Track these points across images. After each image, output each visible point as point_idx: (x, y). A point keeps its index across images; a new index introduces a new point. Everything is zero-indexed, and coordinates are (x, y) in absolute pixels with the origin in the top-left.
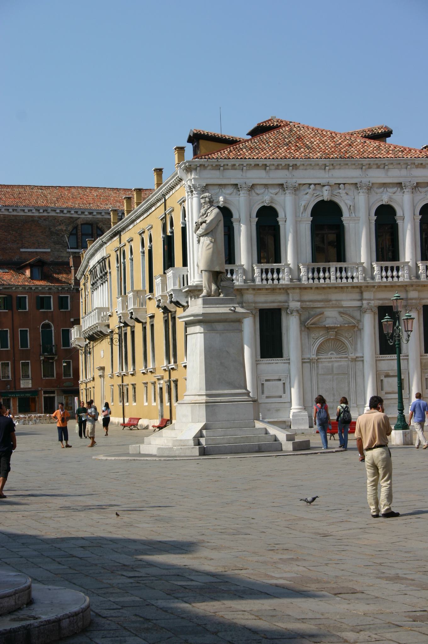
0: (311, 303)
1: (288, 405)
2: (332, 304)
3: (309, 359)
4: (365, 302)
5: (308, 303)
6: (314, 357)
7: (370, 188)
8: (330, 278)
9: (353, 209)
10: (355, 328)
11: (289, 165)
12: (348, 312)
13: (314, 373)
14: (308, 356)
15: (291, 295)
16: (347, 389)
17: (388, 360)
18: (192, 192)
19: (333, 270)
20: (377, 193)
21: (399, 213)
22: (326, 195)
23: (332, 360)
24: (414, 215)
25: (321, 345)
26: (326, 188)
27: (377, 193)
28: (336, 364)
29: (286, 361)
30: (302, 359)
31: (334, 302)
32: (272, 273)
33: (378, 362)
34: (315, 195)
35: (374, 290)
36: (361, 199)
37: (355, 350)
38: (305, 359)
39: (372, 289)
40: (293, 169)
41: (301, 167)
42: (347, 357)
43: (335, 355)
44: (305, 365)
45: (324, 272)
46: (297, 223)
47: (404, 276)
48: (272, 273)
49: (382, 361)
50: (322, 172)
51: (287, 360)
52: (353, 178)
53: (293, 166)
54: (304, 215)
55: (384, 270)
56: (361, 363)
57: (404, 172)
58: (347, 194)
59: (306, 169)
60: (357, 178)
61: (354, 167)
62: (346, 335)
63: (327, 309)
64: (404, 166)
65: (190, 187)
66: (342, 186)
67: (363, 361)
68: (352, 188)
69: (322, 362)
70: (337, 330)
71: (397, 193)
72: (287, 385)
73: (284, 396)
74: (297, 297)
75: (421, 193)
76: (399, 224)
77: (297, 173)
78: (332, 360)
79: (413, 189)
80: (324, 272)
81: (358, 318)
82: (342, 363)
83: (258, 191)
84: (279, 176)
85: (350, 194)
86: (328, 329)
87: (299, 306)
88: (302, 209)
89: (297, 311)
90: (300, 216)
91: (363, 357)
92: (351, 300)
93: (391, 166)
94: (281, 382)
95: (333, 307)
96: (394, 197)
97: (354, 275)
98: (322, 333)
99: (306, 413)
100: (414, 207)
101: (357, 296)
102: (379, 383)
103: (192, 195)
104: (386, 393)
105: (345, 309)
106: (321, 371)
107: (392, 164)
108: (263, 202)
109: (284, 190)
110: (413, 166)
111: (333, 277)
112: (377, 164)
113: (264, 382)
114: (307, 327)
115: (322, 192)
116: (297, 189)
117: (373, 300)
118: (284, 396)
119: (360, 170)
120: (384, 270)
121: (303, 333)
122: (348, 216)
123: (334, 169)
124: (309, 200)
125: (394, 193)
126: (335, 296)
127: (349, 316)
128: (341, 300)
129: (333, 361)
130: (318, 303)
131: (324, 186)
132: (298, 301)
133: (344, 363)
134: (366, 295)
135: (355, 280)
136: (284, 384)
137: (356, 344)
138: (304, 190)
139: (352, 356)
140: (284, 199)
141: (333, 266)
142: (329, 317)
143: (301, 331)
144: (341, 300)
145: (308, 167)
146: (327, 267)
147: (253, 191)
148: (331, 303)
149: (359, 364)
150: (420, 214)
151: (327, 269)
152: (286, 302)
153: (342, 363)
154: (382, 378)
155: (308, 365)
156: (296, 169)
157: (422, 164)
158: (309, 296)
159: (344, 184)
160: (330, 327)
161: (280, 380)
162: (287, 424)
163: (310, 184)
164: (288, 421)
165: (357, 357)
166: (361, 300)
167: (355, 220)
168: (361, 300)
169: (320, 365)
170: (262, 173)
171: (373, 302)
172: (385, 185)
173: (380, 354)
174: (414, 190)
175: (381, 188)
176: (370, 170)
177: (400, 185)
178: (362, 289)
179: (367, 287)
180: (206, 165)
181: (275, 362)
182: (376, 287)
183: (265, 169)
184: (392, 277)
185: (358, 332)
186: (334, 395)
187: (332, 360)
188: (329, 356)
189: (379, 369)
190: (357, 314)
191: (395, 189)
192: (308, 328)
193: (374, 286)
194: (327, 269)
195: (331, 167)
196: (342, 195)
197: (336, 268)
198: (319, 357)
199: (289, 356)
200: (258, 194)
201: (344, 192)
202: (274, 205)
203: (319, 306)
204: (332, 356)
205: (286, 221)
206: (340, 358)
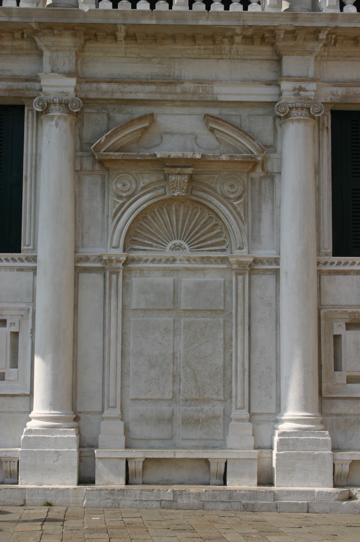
0: (114, 86)
1: (20, 403)
2: (184, 92)
3: (100, 259)
4: (286, 86)
5: (104, 86)
6: (119, 251)
10: (257, 168)
12: (236, 120)
13: (115, 305)
14: (99, 251)
15: (47, 54)
16: (220, 362)
23: (177, 265)
25: (142, 217)
28: (187, 281)
30: (78, 260)
31: (188, 86)
33: (325, 278)
35: (318, 48)
37: (254, 238)
38: (87, 259)
39: (310, 45)
42: (224, 260)
43: (188, 253)
44: (85, 278)
49: (340, 278)
51: (28, 259)
56: (271, 279)
62: (226, 188)
63: (168, 109)
67: (277, 272)
69: (141, 270)
70: (194, 170)
72: (24, 341)
73: (11, 373)
74: (66, 61)
78: (177, 265)
81: (268, 138)
82: (209, 278)
86: (166, 165)
87: (72, 90)
89: (64, 104)
91: (277, 261)
92: (244, 81)
94: (8, 330)
95: (185, 103)
98: (145, 180)
99: (72, 435)
101: (265, 71)
102: (328, 347)
104: (350, 380)
105: (226, 111)
106: (136, 301)
114: (96, 160)
117: (313, 80)
118: (11, 373)
121: (87, 180)
126: (193, 68)
127: (239, 129)
128: (211, 82)
129: (178, 270)
130: (139, 87)
132: (69, 74)
133: (214, 277)
134: (292, 65)
136: (15, 335)
137: (257, 219)
139: (243, 255)
142: (172, 134)
143: (78, 173)
144: (211, 82)
148: (179, 89)
149: (263, 283)
152: (36, 79)
153: (209, 278)
154: (339, 329)
155: (97, 278)
158: (112, 64)
160: (169, 159)
162: (6, 466)
164: (9, 460)
165: (255, 261)
166: (275, 83)
168: (275, 83)
169: (136, 281)
171: (312, 86)
173: (335, 254)
178: (280, 44)
179: (293, 33)
182: (322, 36)
185: (266, 184)
186: (175, 378)
187: (171, 268)
188: (168, 253)
189: (327, 301)
190: (262, 126)
192: (101, 162)
193: (317, 31)
198: (134, 254)
203: (141, 96)
204: (176, 254)
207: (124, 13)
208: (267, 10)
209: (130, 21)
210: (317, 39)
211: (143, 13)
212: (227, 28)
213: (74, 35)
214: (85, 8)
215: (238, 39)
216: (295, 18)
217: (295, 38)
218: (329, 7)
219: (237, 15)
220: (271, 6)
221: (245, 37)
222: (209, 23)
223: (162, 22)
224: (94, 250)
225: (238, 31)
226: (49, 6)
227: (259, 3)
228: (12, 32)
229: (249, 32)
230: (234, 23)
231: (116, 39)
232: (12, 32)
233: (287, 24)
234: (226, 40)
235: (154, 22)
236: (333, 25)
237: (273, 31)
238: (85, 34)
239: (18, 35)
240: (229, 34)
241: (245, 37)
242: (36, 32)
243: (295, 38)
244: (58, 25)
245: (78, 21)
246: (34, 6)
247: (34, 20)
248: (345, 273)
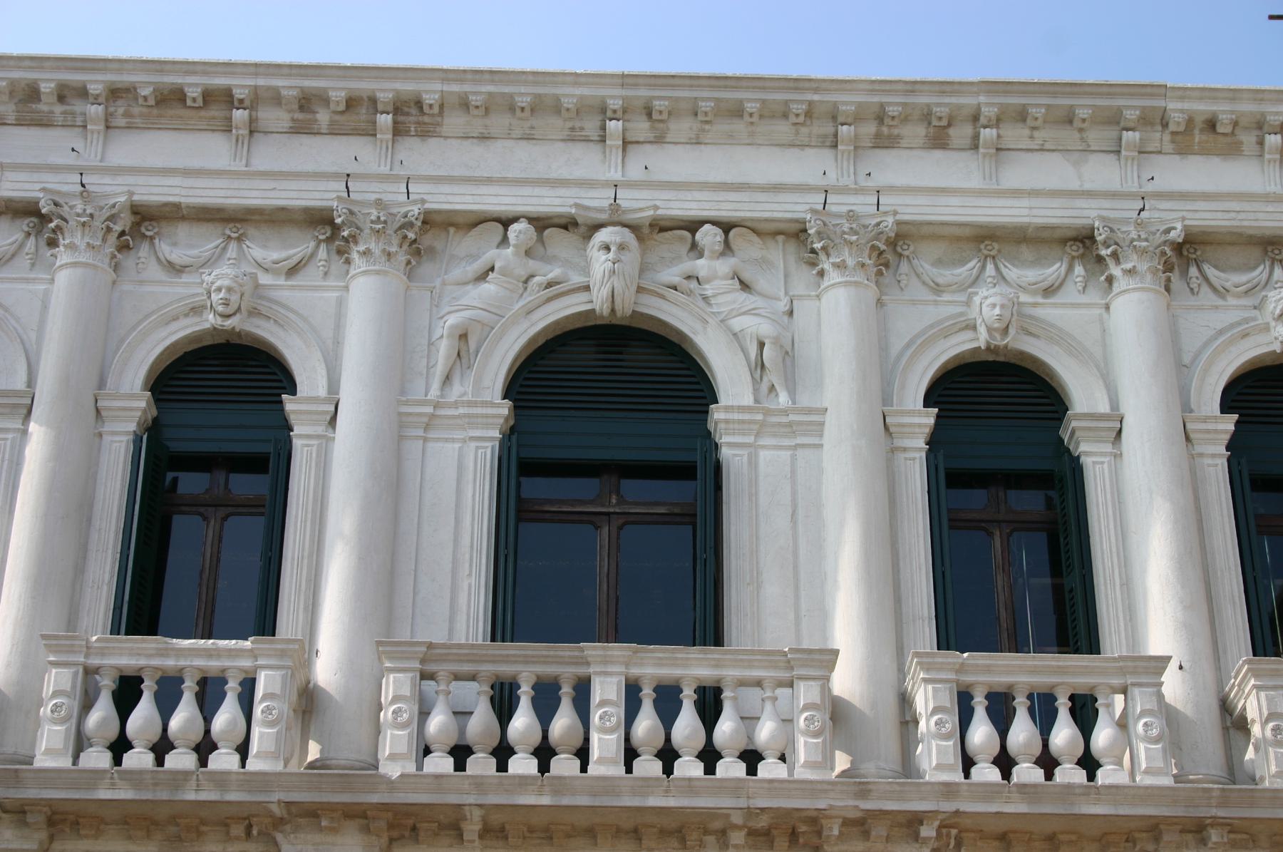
7: (891, 250)
8: (583, 754)
9: (777, 362)
11: (373, 101)
19: (607, 691)
21: (1084, 396)
22: (599, 280)
24: (1186, 408)
26: (603, 235)
27: (937, 289)
36: (833, 313)
40: (398, 131)
41: (454, 122)
45: (545, 706)
46: (402, 429)
47: (1134, 761)
48: (166, 705)
52: (778, 188)
53: (398, 109)
54: (456, 391)
55: (980, 714)
57: (1102, 173)
58: (745, 286)
59: (484, 138)
61: (783, 129)
66: (709, 236)
68: (779, 254)
75: (1221, 292)
76: (1086, 461)
77: (419, 156)
79: (1168, 268)
80: (545, 706)
83: (176, 255)
88: (444, 349)
90: (434, 392)
93: (1014, 134)
96: (1049, 312)
97: (765, 732)
100: (1179, 370)
107: (1022, 116)
109: (340, 252)
110: (1157, 137)
111: (604, 745)
112: (927, 117)
115: (586, 270)
116: (425, 237)
119: (828, 153)
120: (980, 714)
122: (748, 400)
123: (659, 140)
124: (505, 308)
131: (598, 227)
135: (769, 769)
138: (473, 257)
140: (341, 304)
141: (609, 669)
145: (499, 122)
146: (567, 674)
147: (144, 250)
150: (1226, 407)
151: (566, 691)
156: (425, 133)
157: (1211, 125)
159: (726, 227)
163: (506, 222)
167: (792, 429)
170: (211, 150)
172: (989, 241)
174: (1175, 277)
175: (963, 262)
176: (888, 157)
177: (1082, 244)
182: (927, 831)
184: (1048, 762)
191: (1054, 271)
193: (913, 822)
194: (566, 691)
195: (641, 128)
196: (709, 290)
200: (175, 269)
201: (724, 266)
205: (333, 421)
207: (479, 783)
208: (801, 773)
209: (493, 799)
210: (916, 837)
211: (523, 780)
212: (712, 814)
213: (366, 830)
214: (392, 770)
215: (737, 838)
216: (863, 791)
217: (866, 835)
218: (939, 767)
219: (733, 786)
220: (808, 765)
221: (752, 833)
222: (671, 802)
223: (565, 801)
225: (737, 819)
226: (312, 766)
227: (783, 758)
228: (225, 824)
229: (762, 822)
230: (725, 802)
231: (460, 837)
232: (225, 824)
233: (847, 804)
234: (710, 839)
235: (545, 800)
236: (948, 806)
237: (815, 820)
238: (391, 826)
239: (237, 830)
240: (717, 825)
241: (752, 833)
242: (279, 823)
243: (866, 835)
244: (330, 808)
245: (375, 798)
246: (279, 767)
247: (275, 797)
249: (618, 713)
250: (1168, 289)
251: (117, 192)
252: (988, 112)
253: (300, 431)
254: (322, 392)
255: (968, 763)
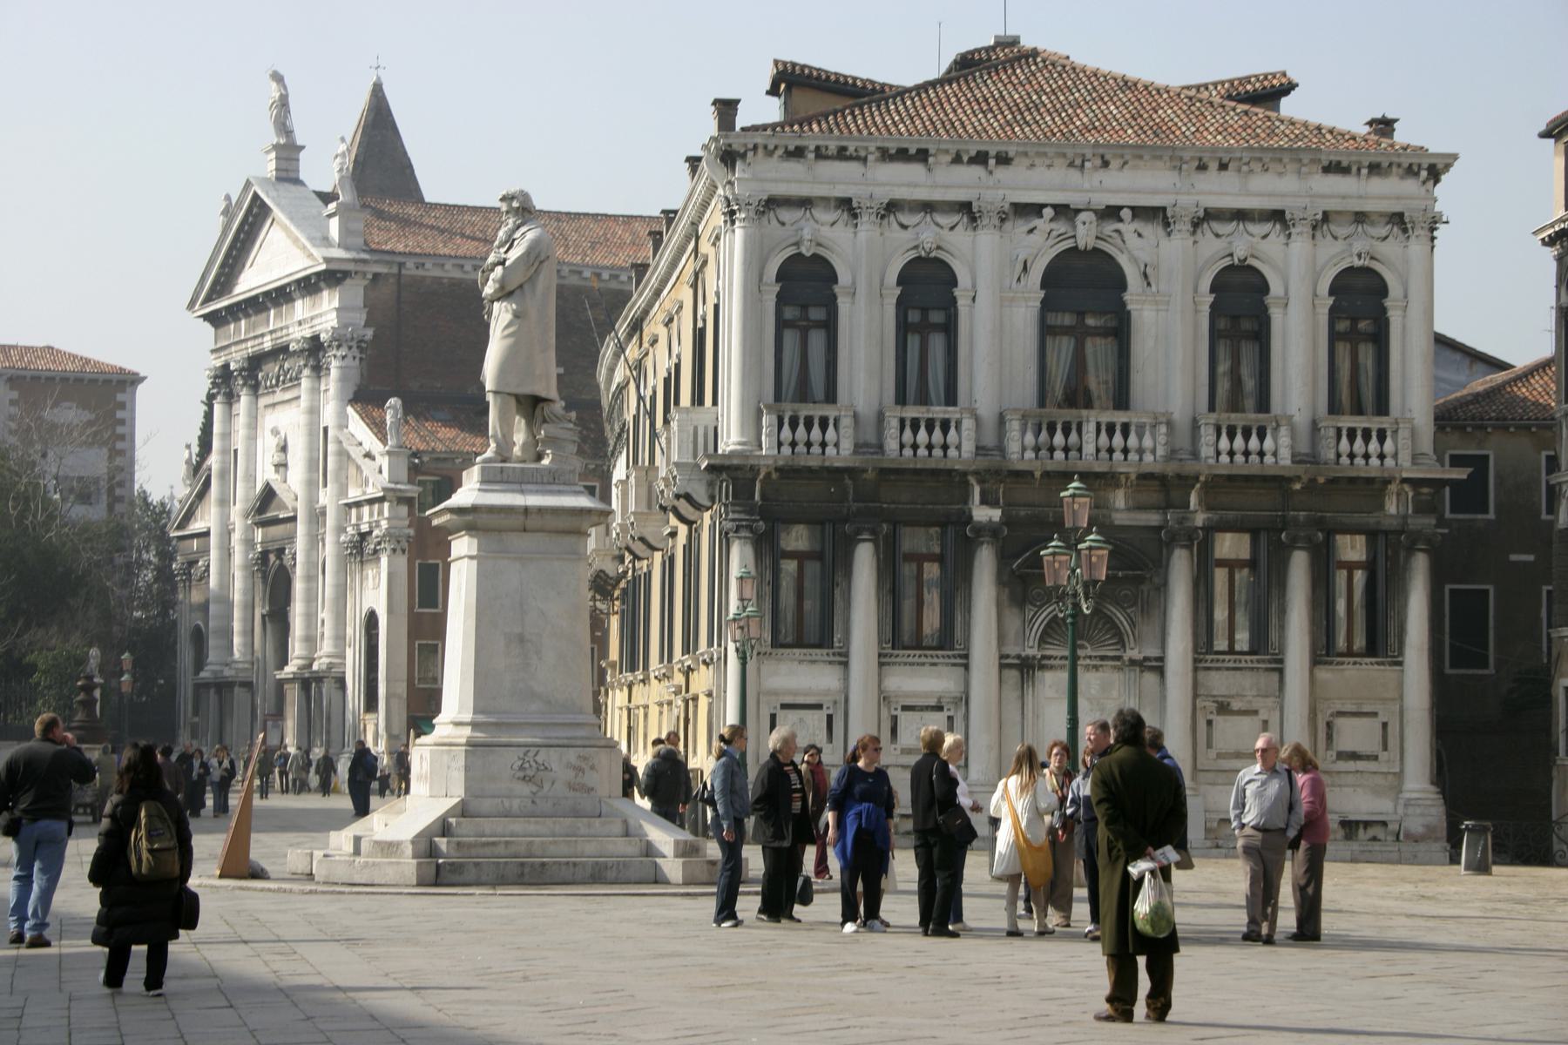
3: (1019, 657)
17: (1228, 669)
18: (732, 213)
19: (1089, 429)
20: (1217, 236)
21: (1276, 288)
24: (1315, 295)
26: (1082, 216)
29: (959, 661)
30: (1002, 657)
32: (930, 430)
33: (1201, 675)
34: (1054, 233)
38: (1008, 656)
42: (1118, 658)
48: (930, 430)
49: (1213, 673)
50: (1074, 175)
58: (1140, 235)
60: (1165, 192)
64: (1256, 166)
65: (727, 199)
71: (840, 224)
80: (1066, 432)
84: (960, 182)
85: (1144, 233)
91: (1161, 659)
94: (946, 714)
96: (1264, 246)
103: (733, 222)
108: (916, 247)
111: (1089, 449)
113: (899, 713)
115: (1074, 227)
119: (1176, 173)
124: (1039, 245)
125: (1265, 237)
161: (939, 708)
165: (1146, 659)
170: (915, 171)
176: (1202, 176)
177: (1277, 216)
180: (771, 147)
181: (930, 660)
183: (925, 161)
194: (1074, 427)
197: (1098, 425)
199: (967, 647)
200: (904, 227)
202: (821, 251)
205: (974, 299)
206: (1103, 658)
224: (1012, 650)
248: (1218, 669)
249: (1093, 435)
250: (1313, 237)
251: (884, 195)
252: (1245, 160)
253: (963, 304)
254: (969, 285)
255: (1218, 453)
